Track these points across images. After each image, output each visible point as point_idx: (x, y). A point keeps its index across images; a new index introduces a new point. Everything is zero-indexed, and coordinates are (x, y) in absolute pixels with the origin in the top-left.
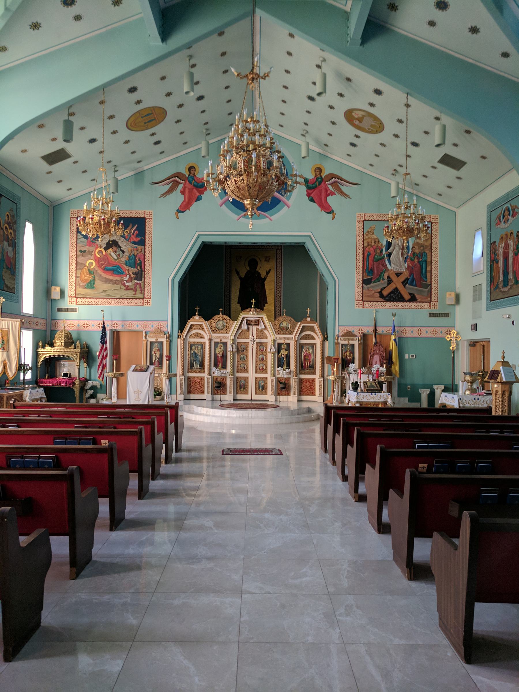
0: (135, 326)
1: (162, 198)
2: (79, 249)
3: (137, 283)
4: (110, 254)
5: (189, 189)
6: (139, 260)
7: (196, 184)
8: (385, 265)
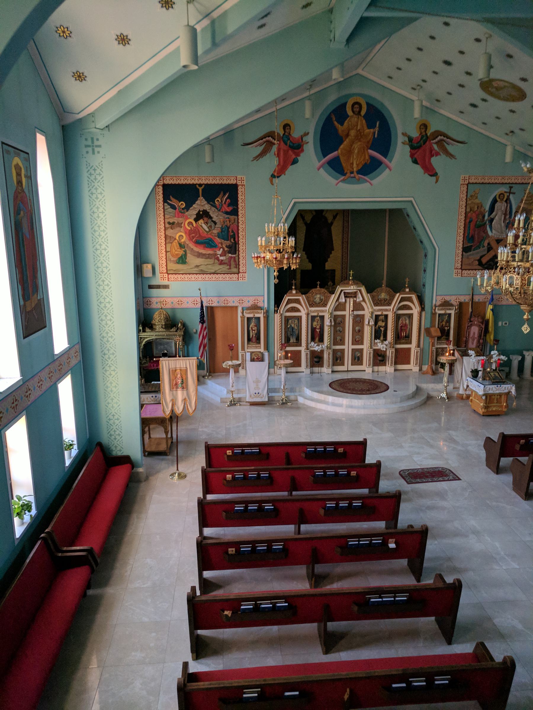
0: (231, 302)
1: (255, 161)
2: (167, 221)
3: (231, 257)
4: (201, 226)
5: (284, 150)
6: (233, 232)
7: (291, 144)
8: (485, 231)
